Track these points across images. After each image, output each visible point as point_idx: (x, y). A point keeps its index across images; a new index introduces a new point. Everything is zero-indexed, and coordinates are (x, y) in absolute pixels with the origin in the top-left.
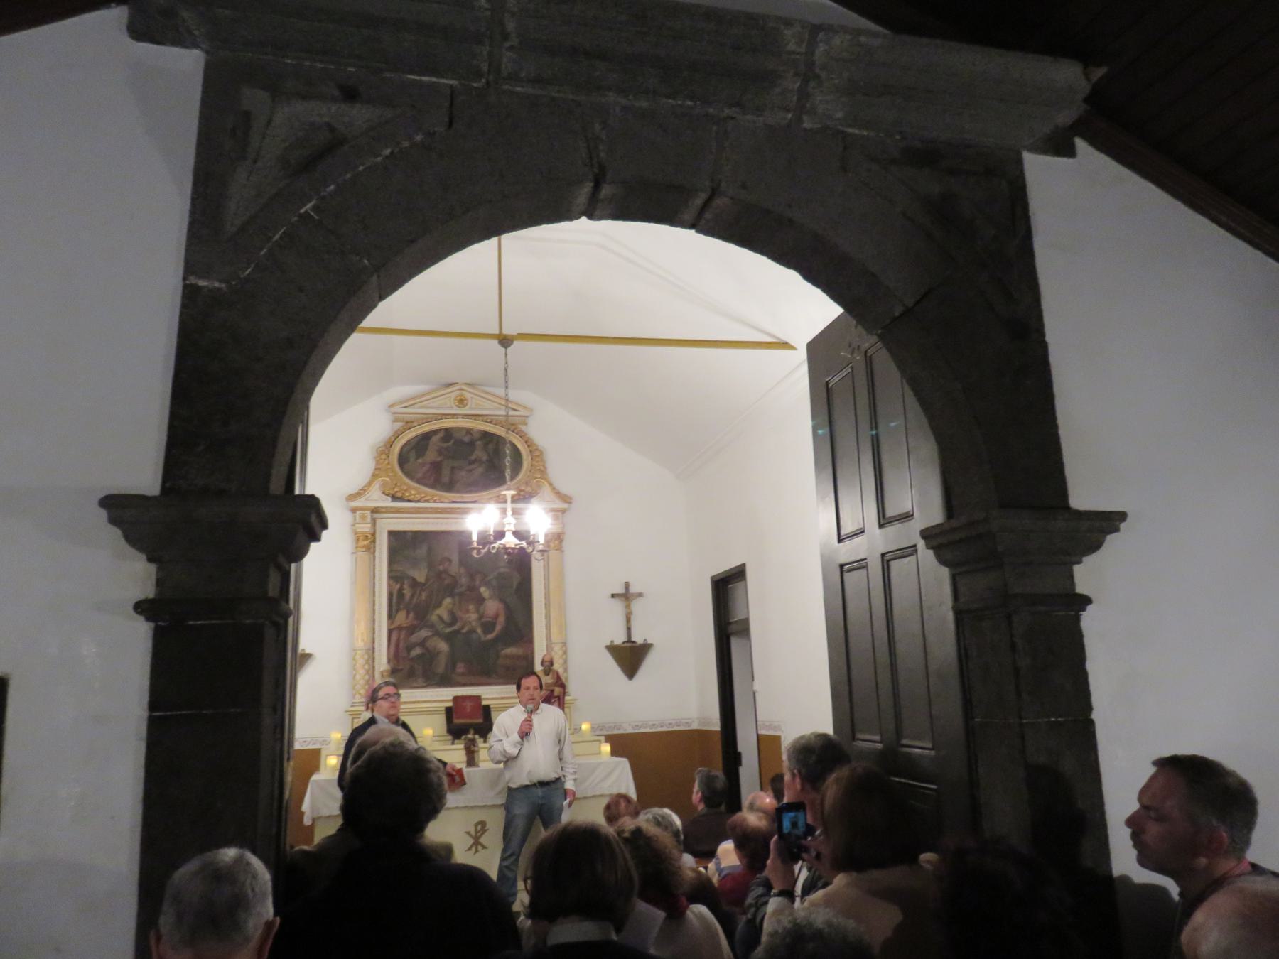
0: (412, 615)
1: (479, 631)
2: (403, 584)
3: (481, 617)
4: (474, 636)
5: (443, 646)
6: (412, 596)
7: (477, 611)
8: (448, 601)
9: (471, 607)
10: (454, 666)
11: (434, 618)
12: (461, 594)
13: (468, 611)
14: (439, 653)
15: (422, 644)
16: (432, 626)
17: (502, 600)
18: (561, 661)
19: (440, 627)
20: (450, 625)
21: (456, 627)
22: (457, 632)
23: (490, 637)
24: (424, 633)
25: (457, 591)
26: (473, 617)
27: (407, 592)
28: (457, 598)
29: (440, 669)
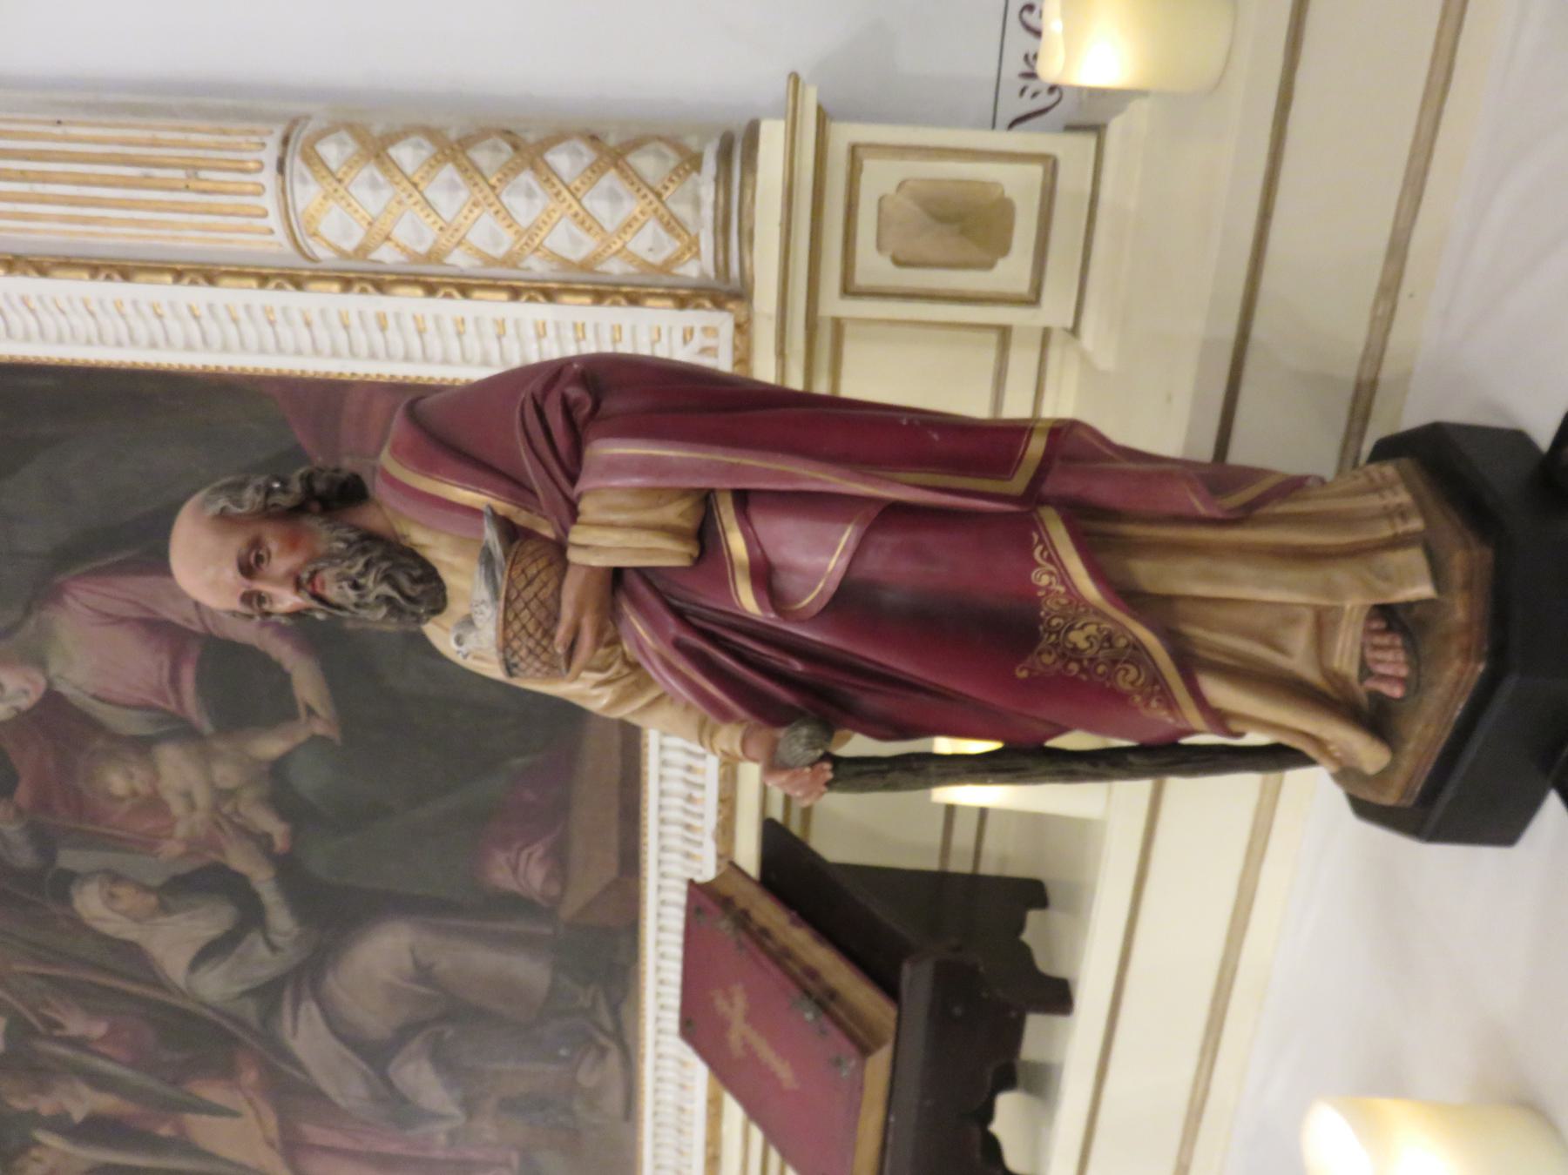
0: (213, 1093)
1: (271, 746)
2: (35, 1119)
3: (183, 732)
4: (309, 780)
5: (384, 954)
6: (100, 1082)
7: (143, 746)
8: (90, 903)
9: (117, 781)
10: (516, 904)
11: (215, 986)
12: (45, 841)
13: (154, 804)
14: (423, 973)
15: (374, 1055)
16: (269, 994)
17: (44, 591)
18: (448, 193)
19: (261, 960)
20: (251, 915)
21: (263, 880)
22: (287, 868)
23: (307, 682)
24: (307, 1038)
25: (25, 857)
26: (176, 769)
27: (82, 1102)
28: (68, 859)
29: (530, 972)
